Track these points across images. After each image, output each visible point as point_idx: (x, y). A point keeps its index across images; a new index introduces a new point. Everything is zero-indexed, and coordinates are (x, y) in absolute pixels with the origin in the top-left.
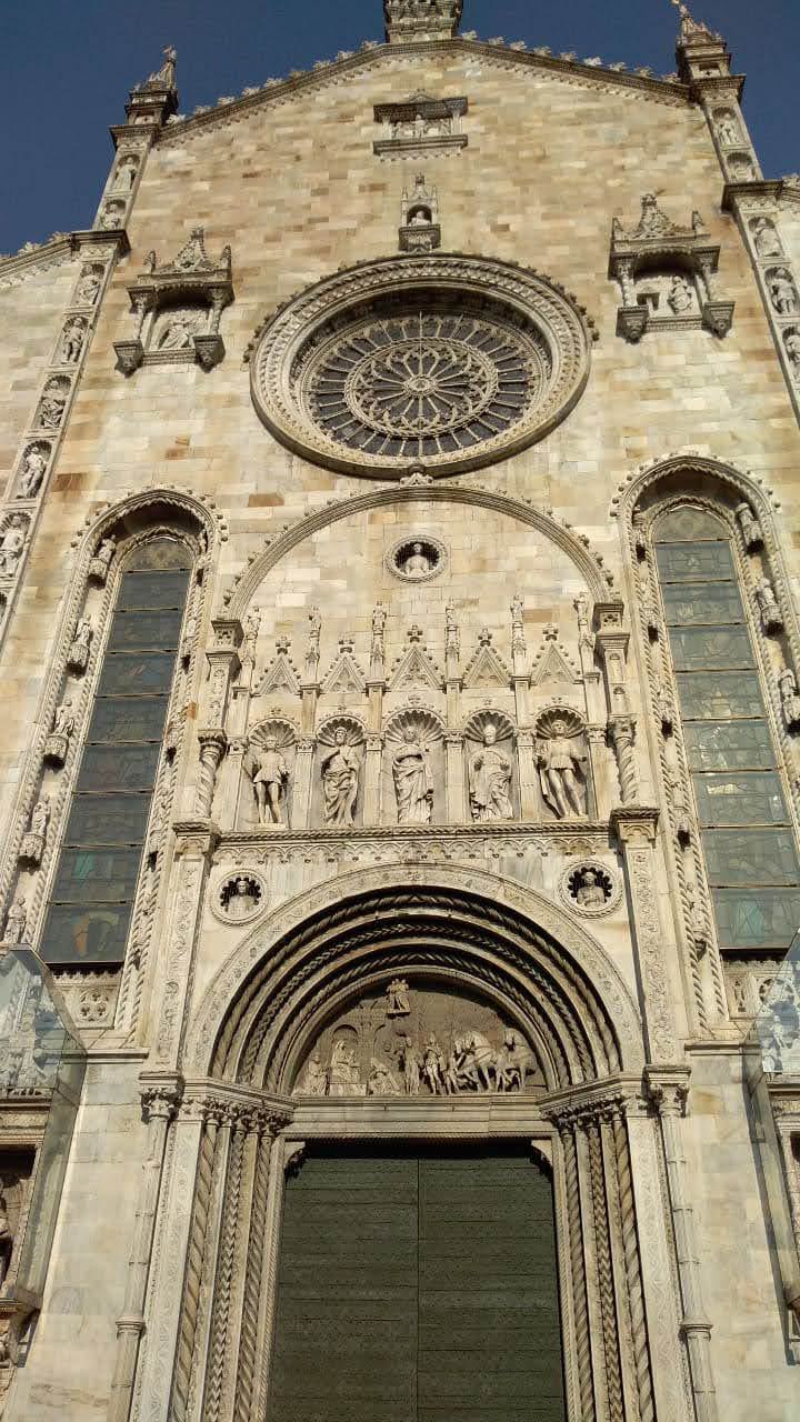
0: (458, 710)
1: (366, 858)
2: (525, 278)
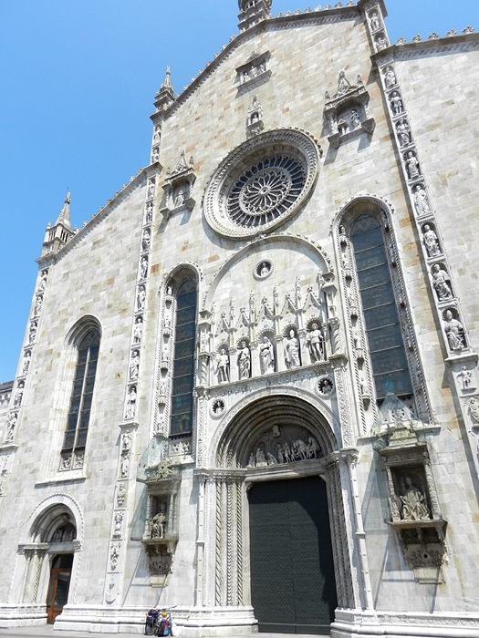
0: (280, 328)
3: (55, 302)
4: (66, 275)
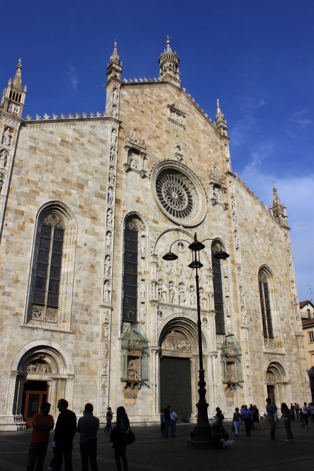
1: (177, 310)
2: (197, 179)
3: (22, 167)
4: (34, 149)
